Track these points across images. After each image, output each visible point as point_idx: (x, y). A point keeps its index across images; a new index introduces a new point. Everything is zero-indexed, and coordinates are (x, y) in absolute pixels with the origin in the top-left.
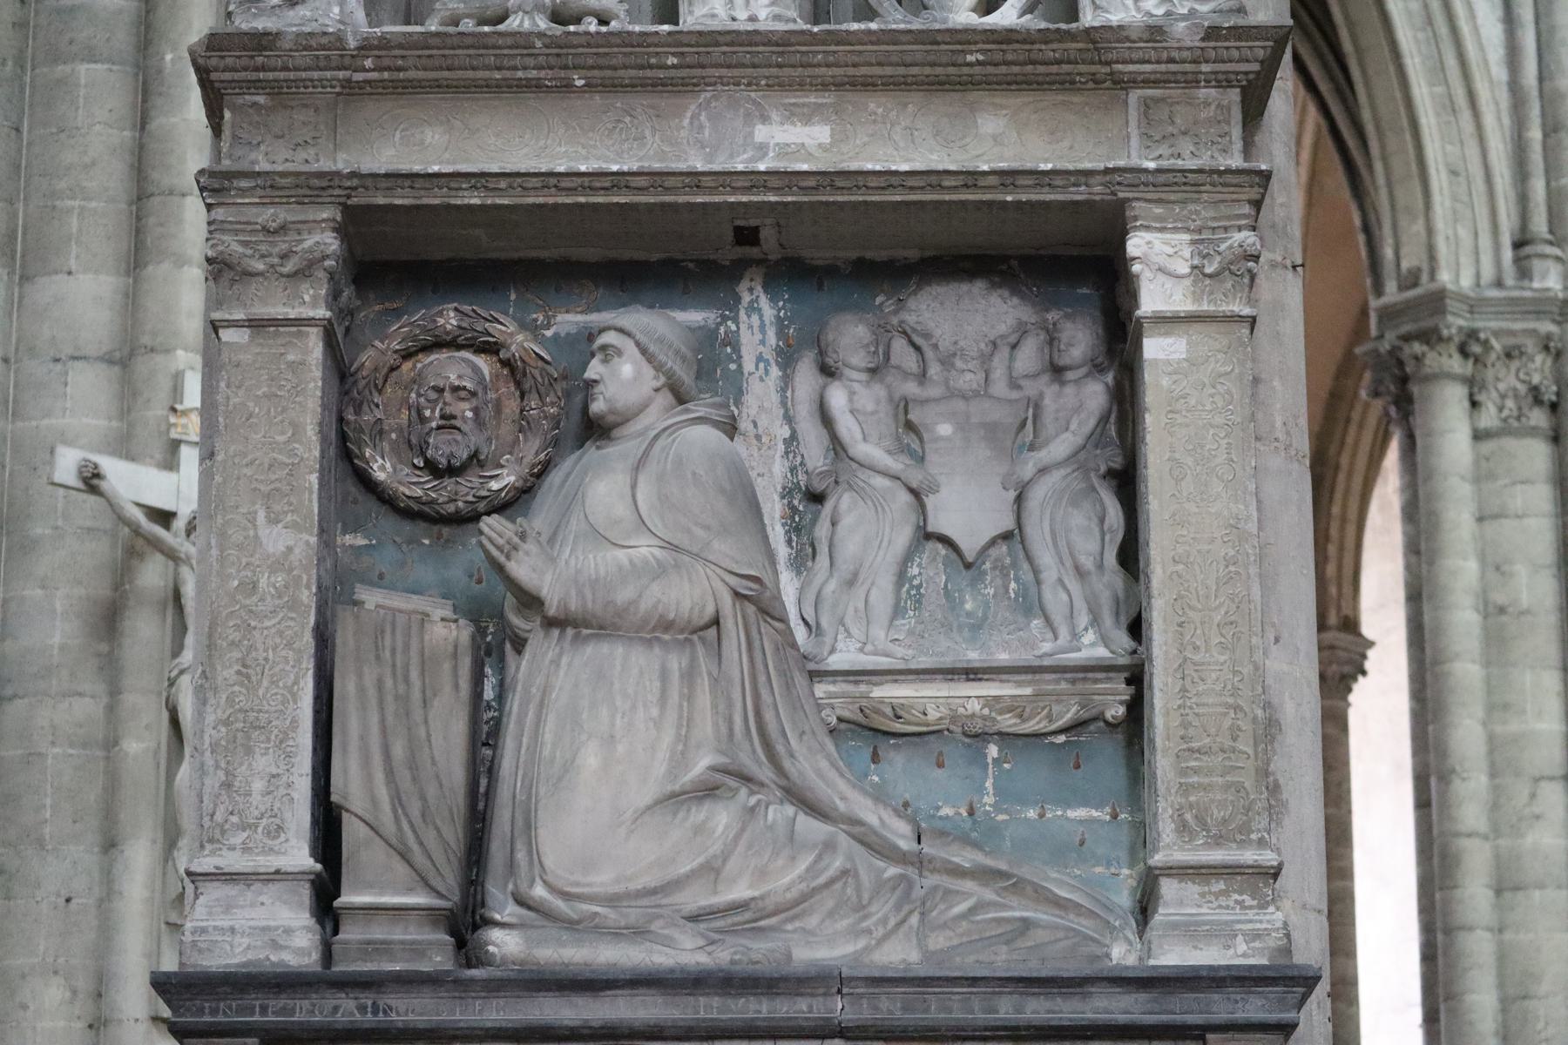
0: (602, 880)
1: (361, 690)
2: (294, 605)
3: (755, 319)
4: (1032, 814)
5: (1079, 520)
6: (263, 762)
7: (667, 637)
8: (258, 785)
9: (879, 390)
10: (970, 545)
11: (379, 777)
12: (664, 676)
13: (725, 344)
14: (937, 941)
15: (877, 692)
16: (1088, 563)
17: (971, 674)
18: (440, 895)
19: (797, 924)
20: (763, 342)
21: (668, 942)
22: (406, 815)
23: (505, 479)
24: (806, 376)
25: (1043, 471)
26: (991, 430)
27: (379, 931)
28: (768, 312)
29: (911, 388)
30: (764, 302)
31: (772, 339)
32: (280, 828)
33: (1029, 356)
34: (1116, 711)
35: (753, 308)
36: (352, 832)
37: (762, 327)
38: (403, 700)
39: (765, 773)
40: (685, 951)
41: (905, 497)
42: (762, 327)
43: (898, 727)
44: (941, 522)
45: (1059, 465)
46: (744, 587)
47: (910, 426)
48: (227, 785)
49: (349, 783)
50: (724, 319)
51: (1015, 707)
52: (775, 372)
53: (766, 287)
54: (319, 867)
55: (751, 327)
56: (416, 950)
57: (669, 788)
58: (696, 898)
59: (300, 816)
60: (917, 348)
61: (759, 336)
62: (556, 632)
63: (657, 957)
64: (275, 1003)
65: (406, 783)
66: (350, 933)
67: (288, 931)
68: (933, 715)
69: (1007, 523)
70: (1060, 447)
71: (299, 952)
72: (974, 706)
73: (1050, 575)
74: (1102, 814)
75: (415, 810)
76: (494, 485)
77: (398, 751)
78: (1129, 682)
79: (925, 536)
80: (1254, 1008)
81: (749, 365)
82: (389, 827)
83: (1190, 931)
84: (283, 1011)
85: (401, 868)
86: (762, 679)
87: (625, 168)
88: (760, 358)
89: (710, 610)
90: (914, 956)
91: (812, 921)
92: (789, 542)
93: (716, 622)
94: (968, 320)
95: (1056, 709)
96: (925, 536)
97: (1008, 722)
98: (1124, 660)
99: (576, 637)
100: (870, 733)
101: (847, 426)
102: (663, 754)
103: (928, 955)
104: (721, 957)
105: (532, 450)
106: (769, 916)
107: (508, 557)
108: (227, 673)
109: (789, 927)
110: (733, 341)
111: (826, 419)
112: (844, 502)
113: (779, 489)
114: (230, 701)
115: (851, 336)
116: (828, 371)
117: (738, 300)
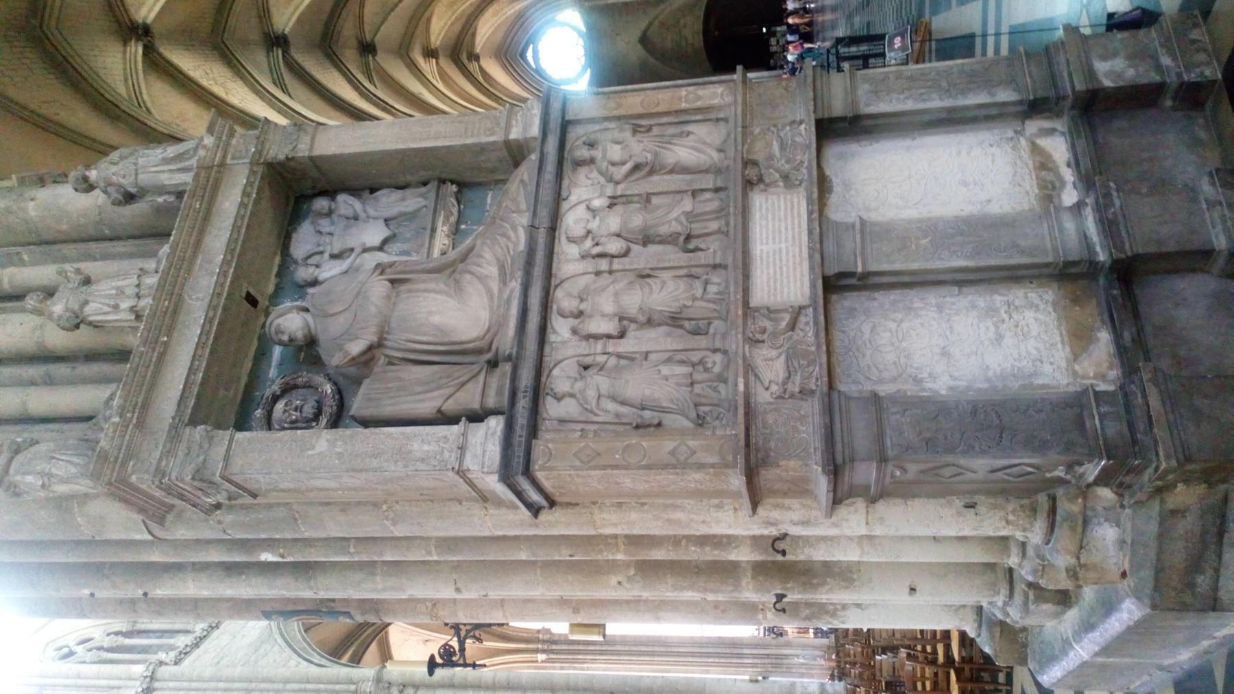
1: (392, 404)
2: (352, 437)
5: (384, 200)
6: (416, 446)
8: (426, 447)
11: (429, 395)
14: (523, 206)
17: (433, 230)
21: (512, 291)
25: (365, 211)
26: (347, 227)
27: (492, 392)
29: (326, 256)
32: (445, 437)
33: (325, 224)
34: (454, 188)
38: (398, 389)
40: (515, 286)
41: (366, 255)
48: (423, 460)
51: (447, 218)
63: (517, 293)
65: (433, 385)
66: (491, 402)
67: (488, 429)
69: (381, 222)
70: (357, 205)
71: (497, 424)
72: (445, 229)
77: (420, 389)
82: (450, 390)
84: (522, 428)
85: (469, 385)
91: (511, 246)
93: (392, 281)
97: (453, 219)
99: (388, 333)
102: (438, 296)
103: (528, 209)
104: (519, 274)
108: (375, 463)
114: (387, 461)
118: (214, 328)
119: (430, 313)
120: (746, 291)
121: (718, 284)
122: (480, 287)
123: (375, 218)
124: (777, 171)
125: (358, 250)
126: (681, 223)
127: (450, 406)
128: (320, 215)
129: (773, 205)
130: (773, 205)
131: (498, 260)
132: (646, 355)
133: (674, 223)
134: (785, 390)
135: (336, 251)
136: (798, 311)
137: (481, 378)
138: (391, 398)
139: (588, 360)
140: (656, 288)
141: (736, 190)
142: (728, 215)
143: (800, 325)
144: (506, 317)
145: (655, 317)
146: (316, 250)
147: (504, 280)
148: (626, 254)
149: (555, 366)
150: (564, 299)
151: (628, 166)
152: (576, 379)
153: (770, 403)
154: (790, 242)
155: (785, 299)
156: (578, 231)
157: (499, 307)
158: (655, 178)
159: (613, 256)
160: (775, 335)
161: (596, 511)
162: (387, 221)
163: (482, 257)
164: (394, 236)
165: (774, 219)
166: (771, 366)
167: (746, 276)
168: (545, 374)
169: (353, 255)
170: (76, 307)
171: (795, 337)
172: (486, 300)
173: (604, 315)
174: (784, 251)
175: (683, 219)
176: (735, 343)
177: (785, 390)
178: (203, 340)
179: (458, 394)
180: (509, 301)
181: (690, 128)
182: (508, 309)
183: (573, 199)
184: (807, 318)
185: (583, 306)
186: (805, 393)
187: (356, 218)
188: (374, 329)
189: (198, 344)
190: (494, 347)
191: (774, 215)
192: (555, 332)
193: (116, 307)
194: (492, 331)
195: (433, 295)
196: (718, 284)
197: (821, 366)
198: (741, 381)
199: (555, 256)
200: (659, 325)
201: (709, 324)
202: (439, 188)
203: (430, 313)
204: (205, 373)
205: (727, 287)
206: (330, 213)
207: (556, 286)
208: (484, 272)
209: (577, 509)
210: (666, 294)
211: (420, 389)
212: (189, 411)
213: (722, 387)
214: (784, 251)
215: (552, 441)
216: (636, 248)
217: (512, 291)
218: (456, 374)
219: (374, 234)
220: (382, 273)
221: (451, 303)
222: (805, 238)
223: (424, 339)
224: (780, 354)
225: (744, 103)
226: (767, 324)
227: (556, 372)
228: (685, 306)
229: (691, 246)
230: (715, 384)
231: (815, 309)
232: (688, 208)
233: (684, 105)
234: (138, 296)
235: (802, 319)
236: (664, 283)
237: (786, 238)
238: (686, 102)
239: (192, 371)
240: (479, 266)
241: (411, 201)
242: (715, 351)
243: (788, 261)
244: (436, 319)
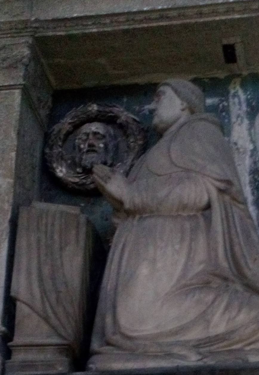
0: (148, 329)
3: (236, 100)
7: (185, 214)
12: (183, 232)
13: (222, 111)
18: (65, 339)
19: (252, 346)
20: (240, 109)
22: (49, 301)
28: (242, 96)
30: (241, 93)
31: (244, 108)
35: (235, 95)
36: (22, 309)
37: (240, 103)
42: (240, 103)
46: (222, 186)
49: (20, 288)
50: (223, 101)
52: (246, 122)
53: (243, 86)
55: (234, 103)
57: (183, 282)
61: (238, 107)
65: (49, 285)
75: (53, 297)
77: (46, 270)
81: (234, 119)
85: (45, 327)
86: (233, 232)
87: (165, 7)
88: (238, 116)
89: (205, 199)
92: (253, 194)
93: (209, 206)
102: (180, 267)
106: (237, 342)
107: (106, 182)
109: (248, 348)
110: (226, 110)
113: (248, 170)
117: (228, 92)
118: (155, 24)
122: (192, 315)
131: (233, 332)
138: (39, 241)
144: (146, 355)
157: (160, 345)
163: (239, 311)
172: (172, 326)
178: (138, 18)
179: (35, 317)
180: (169, 355)
182: (156, 357)
188: (137, 201)
189: (129, 13)
195: (183, 260)
203: (154, 261)
204: (100, 34)
208: (216, 318)
211: (46, 270)
212: (50, 34)
217: (183, 357)
220: (221, 191)
221: (166, 284)
223: (124, 263)
239: (96, 18)
240: (227, 308)
244: (144, 270)
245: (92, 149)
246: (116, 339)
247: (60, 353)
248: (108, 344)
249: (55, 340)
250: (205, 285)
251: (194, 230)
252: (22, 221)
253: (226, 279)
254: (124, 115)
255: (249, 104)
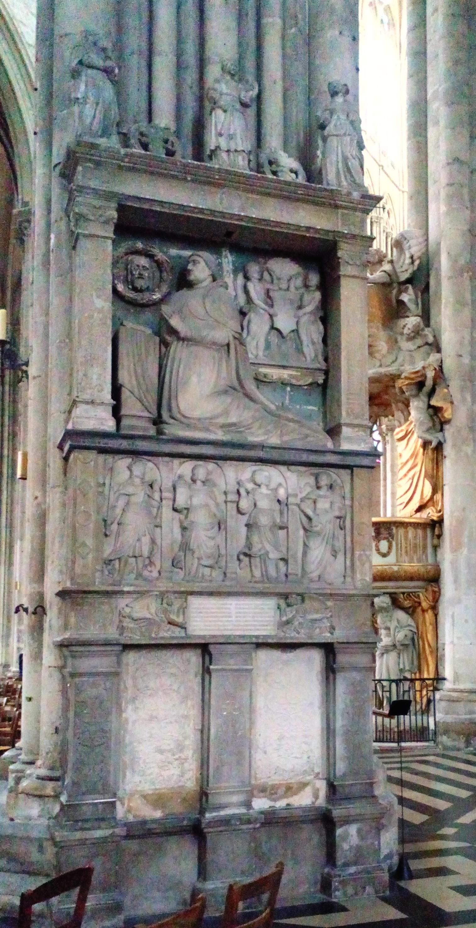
0: (197, 414)
3: (226, 260)
4: (298, 407)
5: (313, 328)
9: (261, 285)
10: (285, 331)
14: (286, 438)
15: (260, 370)
16: (315, 340)
17: (284, 367)
23: (157, 296)
24: (240, 280)
25: (305, 314)
30: (229, 255)
31: (231, 266)
33: (299, 282)
39: (238, 388)
40: (219, 435)
41: (268, 316)
43: (265, 380)
44: (278, 325)
45: (308, 313)
47: (269, 297)
52: (232, 276)
53: (230, 252)
54: (115, 402)
56: (145, 429)
57: (216, 390)
58: (221, 421)
59: (108, 388)
60: (271, 275)
62: (181, 342)
63: (212, 437)
64: (106, 441)
68: (275, 377)
69: (294, 327)
70: (309, 308)
73: (305, 343)
74: (315, 409)
76: (154, 297)
78: (325, 374)
79: (273, 328)
80: (366, 461)
81: (225, 273)
83: (349, 439)
89: (227, 342)
90: (279, 442)
94: (285, 269)
95: (307, 378)
96: (273, 328)
98: (324, 368)
100: (259, 381)
101: (253, 294)
105: (165, 289)
111: (246, 291)
112: (252, 315)
115: (254, 269)
116: (247, 278)
117: (222, 253)
119: (199, 375)
120: (200, 593)
121: (211, 575)
123: (297, 323)
124: (294, 617)
125: (271, 311)
126: (260, 550)
127: (125, 394)
128: (306, 279)
129: (267, 613)
130: (267, 613)
132: (158, 526)
133: (260, 546)
134: (124, 617)
135: (271, 294)
136: (183, 627)
137: (146, 414)
139: (156, 487)
140: (210, 534)
141: (281, 589)
142: (262, 582)
143: (172, 627)
144: (195, 428)
145: (188, 533)
146: (275, 277)
147: (222, 426)
148: (239, 511)
149: (155, 465)
150: (204, 469)
151: (310, 513)
152: (142, 479)
153: (116, 607)
154: (235, 623)
155: (192, 619)
156: (260, 478)
158: (302, 532)
159: (238, 503)
160: (165, 611)
161: (60, 489)
162: (296, 331)
164: (283, 337)
165: (255, 613)
166: (145, 609)
167: (211, 594)
168: (150, 458)
169: (266, 307)
170: (222, 103)
171: (163, 625)
173: (191, 497)
174: (230, 619)
175: (263, 552)
176: (163, 586)
177: (124, 617)
180: (207, 430)
181: (341, 557)
182: (200, 430)
183: (288, 474)
184: (177, 632)
185: (199, 483)
186: (122, 629)
187: (300, 307)
190: (172, 421)
191: (258, 613)
192: (181, 464)
193: (220, 135)
194: (183, 419)
196: (211, 575)
197: (139, 640)
198: (131, 589)
199: (241, 463)
200: (182, 535)
201: (181, 569)
202: (319, 370)
203: (199, 375)
205: (206, 581)
206: (306, 286)
207: (216, 464)
209: (62, 476)
210: (204, 539)
213: (133, 576)
214: (230, 619)
215: (96, 464)
216: (244, 519)
218: (149, 398)
219: (285, 322)
221: (208, 389)
222: (238, 633)
224: (152, 615)
225: (353, 595)
226: (176, 606)
227: (150, 465)
228: (193, 552)
229: (242, 557)
230: (135, 572)
231: (182, 638)
232: (271, 556)
233: (357, 553)
234: (228, 151)
235: (177, 630)
236: (213, 538)
237: (240, 621)
238: (360, 555)
241: (311, 349)
242: (159, 572)
243: (221, 621)
244: (194, 379)
245: (141, 276)
246: (179, 416)
247: (149, 421)
248: (173, 418)
249: (146, 414)
250: (225, 392)
251: (220, 359)
252: (122, 336)
253: (234, 389)
254: (160, 256)
255: (234, 265)
